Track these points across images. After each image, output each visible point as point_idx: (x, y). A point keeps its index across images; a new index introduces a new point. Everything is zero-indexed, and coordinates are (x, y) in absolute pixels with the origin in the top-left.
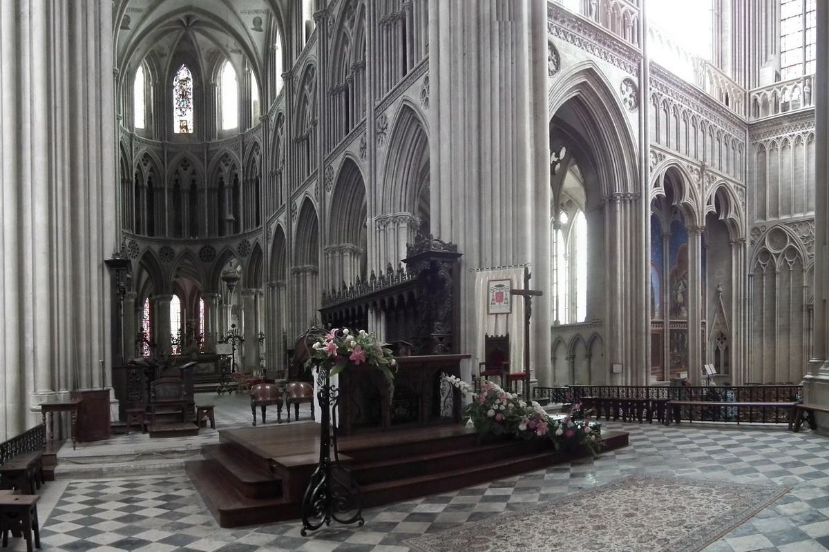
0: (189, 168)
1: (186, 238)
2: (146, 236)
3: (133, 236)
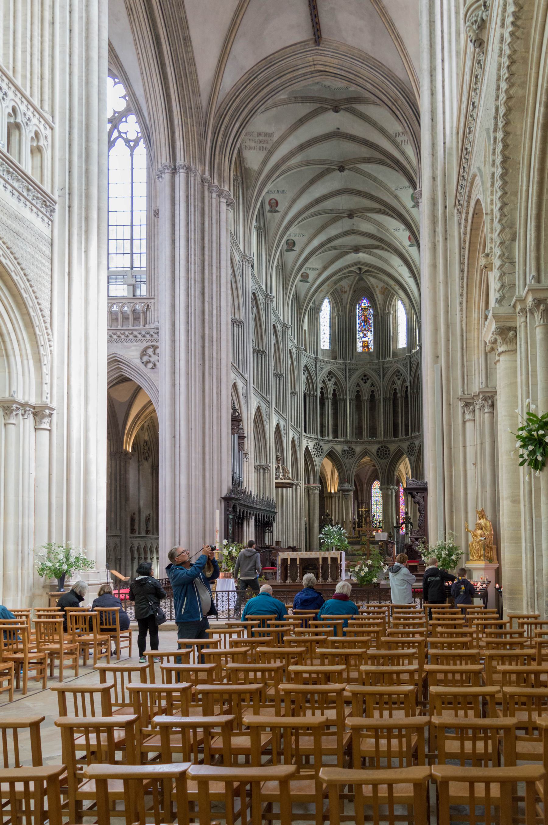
0: (369, 382)
1: (366, 439)
2: (331, 438)
3: (317, 439)
